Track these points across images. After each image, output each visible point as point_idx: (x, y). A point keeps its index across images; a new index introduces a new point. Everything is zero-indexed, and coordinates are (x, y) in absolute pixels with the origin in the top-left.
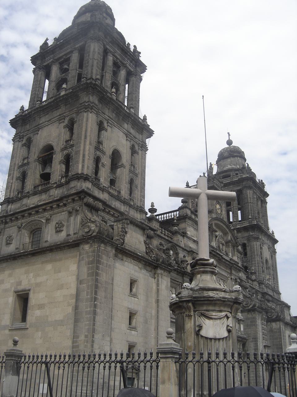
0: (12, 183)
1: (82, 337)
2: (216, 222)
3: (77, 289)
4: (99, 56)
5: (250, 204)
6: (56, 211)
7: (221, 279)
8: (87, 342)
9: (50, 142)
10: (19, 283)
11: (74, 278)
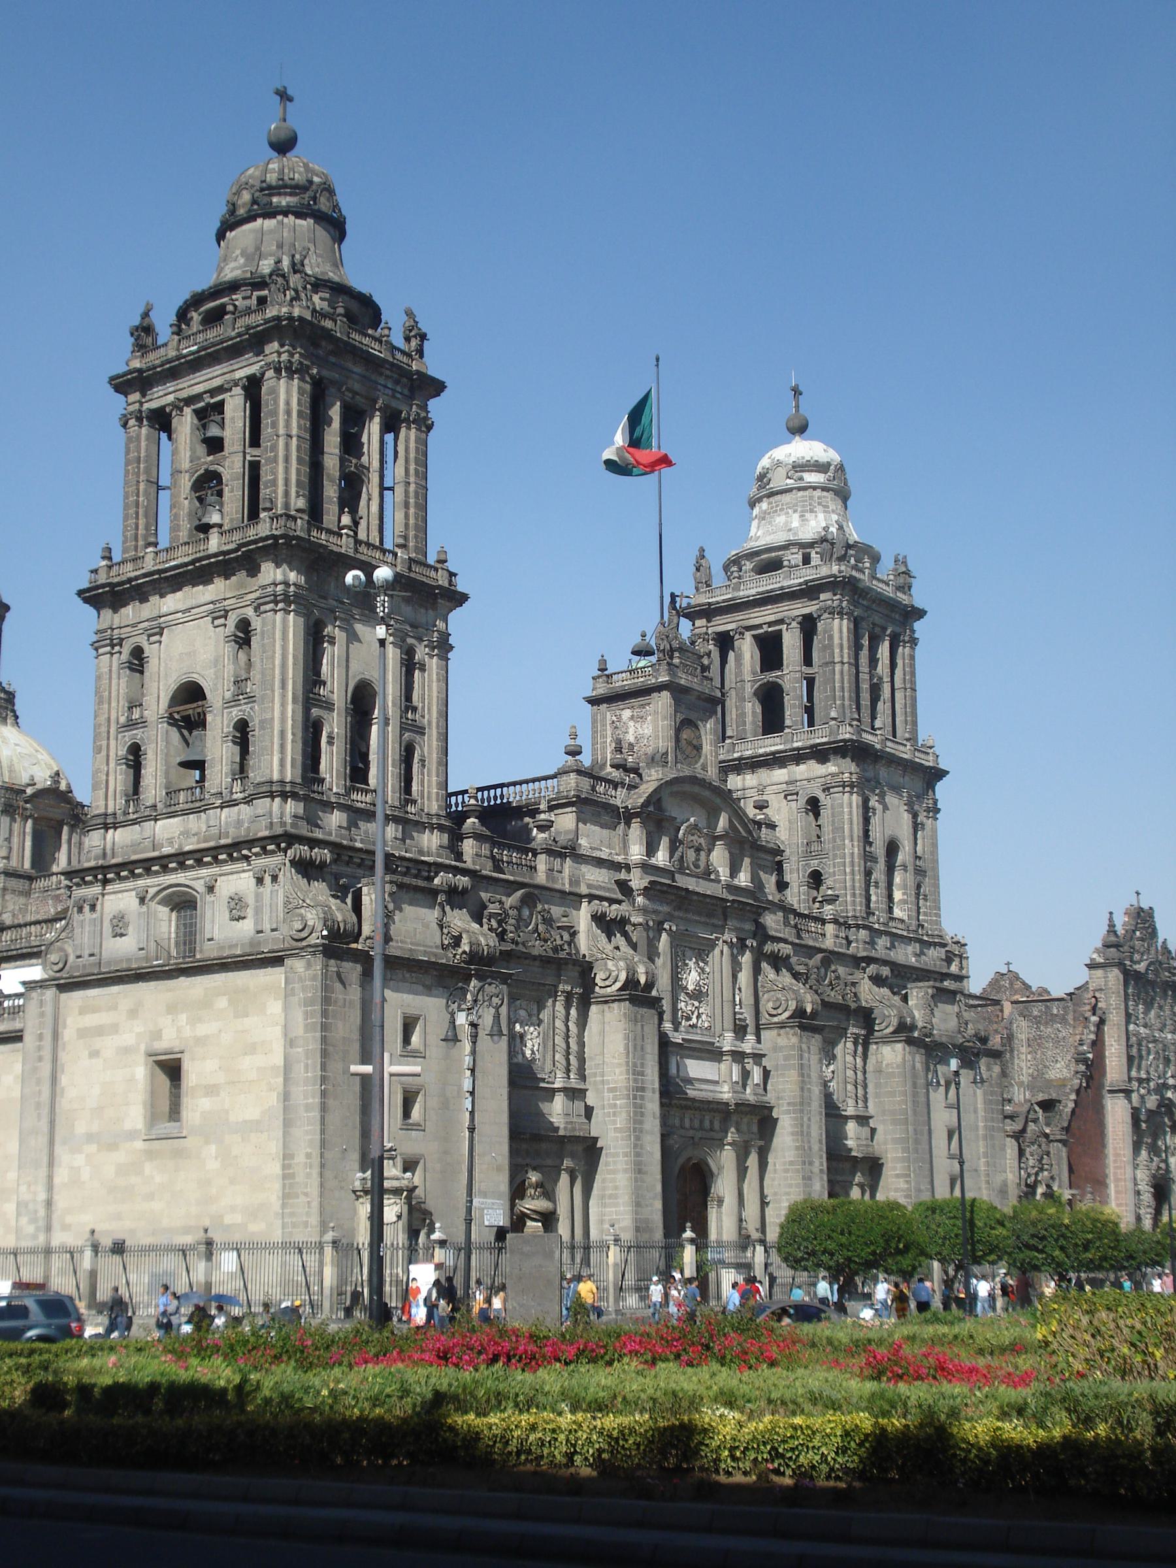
0: (107, 775)
1: (300, 1158)
2: (675, 788)
3: (285, 1058)
4: (302, 422)
5: (838, 667)
6: (227, 868)
7: (690, 948)
8: (311, 1167)
9: (194, 675)
10: (157, 1035)
11: (278, 1031)
